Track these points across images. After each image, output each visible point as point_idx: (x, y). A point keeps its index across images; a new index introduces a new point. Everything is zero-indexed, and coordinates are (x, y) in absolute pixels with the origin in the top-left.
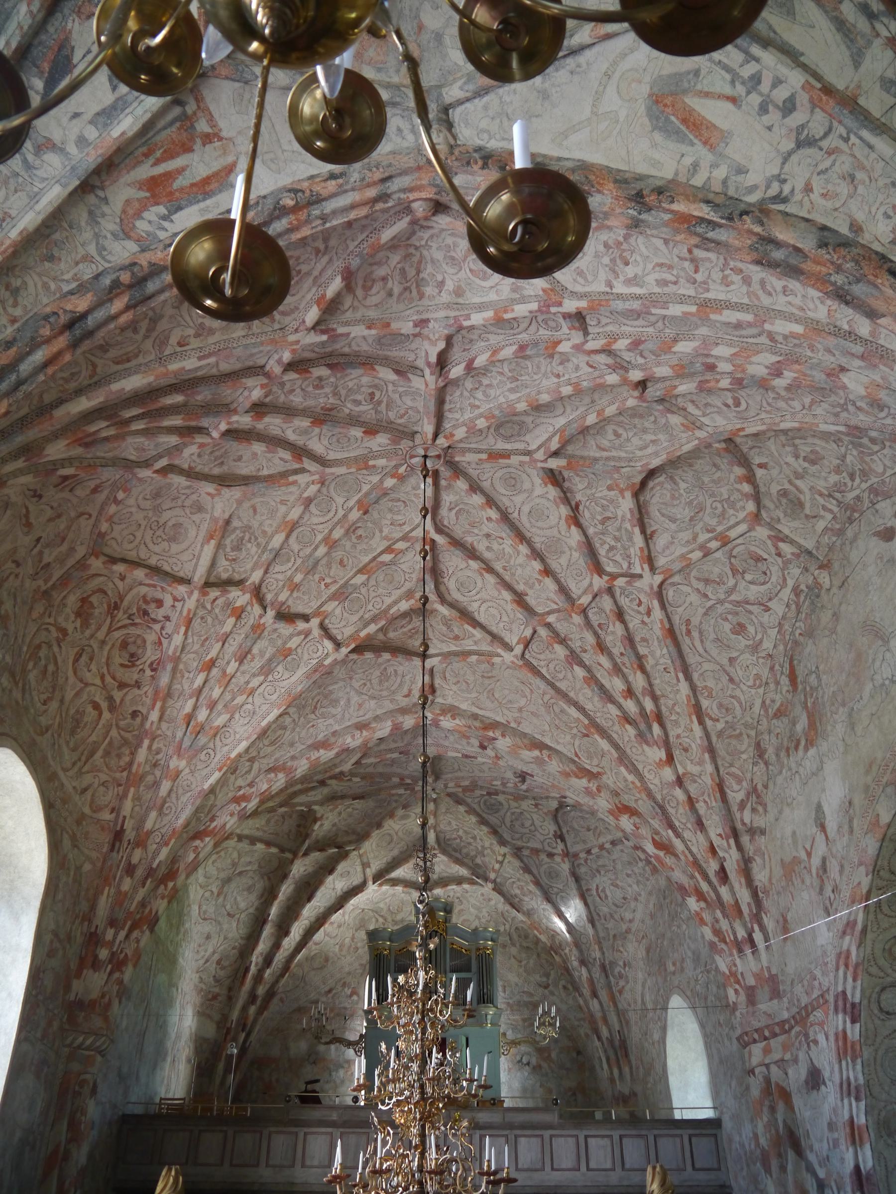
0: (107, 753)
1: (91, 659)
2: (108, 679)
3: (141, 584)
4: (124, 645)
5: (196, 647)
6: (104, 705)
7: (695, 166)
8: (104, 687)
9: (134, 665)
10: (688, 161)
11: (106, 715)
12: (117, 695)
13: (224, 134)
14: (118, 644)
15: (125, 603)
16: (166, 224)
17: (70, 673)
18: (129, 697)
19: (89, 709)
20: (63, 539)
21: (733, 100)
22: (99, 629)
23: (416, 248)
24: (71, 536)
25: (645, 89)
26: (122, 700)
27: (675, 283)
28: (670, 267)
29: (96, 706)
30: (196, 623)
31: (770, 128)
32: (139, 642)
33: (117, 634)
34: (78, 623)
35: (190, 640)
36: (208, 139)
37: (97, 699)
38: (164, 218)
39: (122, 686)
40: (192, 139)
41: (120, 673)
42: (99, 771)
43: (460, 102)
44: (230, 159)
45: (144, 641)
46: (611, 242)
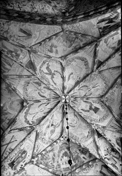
7: (23, 25)
10: (24, 26)
13: (98, 29)
16: (111, 15)
21: (19, 36)
23: (68, 4)
25: (33, 36)
27: (22, 2)
28: (23, 5)
31: (12, 33)
36: (101, 28)
38: (111, 16)
40: (103, 28)
43: (61, 32)
44: (98, 25)
46: (34, 9)
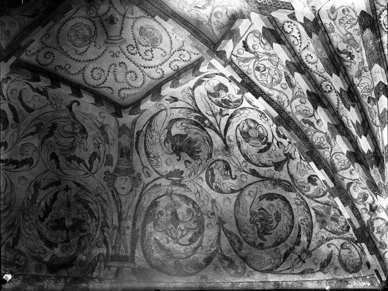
0: (323, 224)
1: (228, 168)
2: (261, 170)
3: (193, 89)
4: (246, 135)
5: (289, 92)
6: (279, 191)
8: (264, 179)
9: (269, 145)
11: (291, 196)
12: (283, 175)
14: (241, 139)
15: (203, 111)
17: (214, 195)
18: (293, 171)
19: (265, 203)
20: (83, 130)
22: (211, 143)
24: (87, 124)
26: (291, 176)
29: (270, 197)
30: (256, 77)
32: (252, 125)
33: (231, 133)
34: (185, 156)
35: (275, 95)
37: (265, 191)
39: (278, 166)
41: (264, 158)
42: (328, 239)
45: (254, 122)
